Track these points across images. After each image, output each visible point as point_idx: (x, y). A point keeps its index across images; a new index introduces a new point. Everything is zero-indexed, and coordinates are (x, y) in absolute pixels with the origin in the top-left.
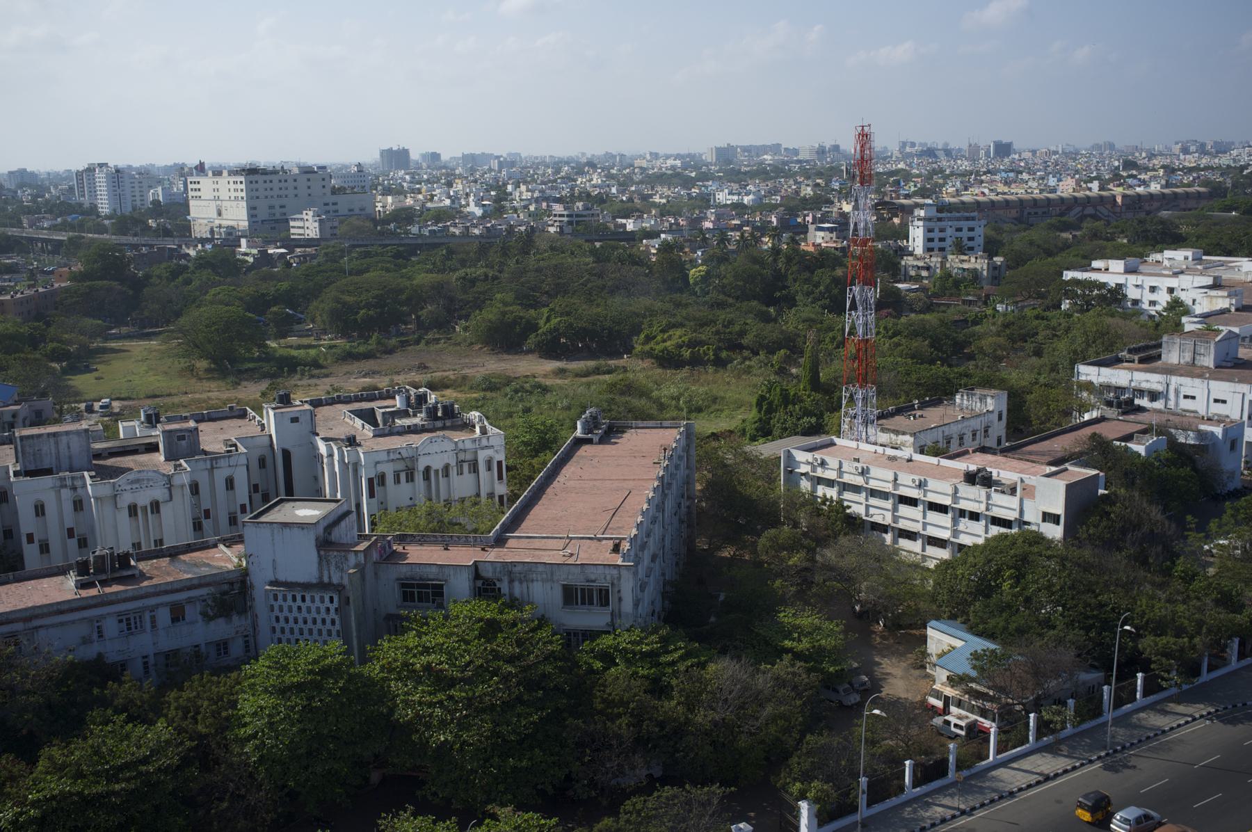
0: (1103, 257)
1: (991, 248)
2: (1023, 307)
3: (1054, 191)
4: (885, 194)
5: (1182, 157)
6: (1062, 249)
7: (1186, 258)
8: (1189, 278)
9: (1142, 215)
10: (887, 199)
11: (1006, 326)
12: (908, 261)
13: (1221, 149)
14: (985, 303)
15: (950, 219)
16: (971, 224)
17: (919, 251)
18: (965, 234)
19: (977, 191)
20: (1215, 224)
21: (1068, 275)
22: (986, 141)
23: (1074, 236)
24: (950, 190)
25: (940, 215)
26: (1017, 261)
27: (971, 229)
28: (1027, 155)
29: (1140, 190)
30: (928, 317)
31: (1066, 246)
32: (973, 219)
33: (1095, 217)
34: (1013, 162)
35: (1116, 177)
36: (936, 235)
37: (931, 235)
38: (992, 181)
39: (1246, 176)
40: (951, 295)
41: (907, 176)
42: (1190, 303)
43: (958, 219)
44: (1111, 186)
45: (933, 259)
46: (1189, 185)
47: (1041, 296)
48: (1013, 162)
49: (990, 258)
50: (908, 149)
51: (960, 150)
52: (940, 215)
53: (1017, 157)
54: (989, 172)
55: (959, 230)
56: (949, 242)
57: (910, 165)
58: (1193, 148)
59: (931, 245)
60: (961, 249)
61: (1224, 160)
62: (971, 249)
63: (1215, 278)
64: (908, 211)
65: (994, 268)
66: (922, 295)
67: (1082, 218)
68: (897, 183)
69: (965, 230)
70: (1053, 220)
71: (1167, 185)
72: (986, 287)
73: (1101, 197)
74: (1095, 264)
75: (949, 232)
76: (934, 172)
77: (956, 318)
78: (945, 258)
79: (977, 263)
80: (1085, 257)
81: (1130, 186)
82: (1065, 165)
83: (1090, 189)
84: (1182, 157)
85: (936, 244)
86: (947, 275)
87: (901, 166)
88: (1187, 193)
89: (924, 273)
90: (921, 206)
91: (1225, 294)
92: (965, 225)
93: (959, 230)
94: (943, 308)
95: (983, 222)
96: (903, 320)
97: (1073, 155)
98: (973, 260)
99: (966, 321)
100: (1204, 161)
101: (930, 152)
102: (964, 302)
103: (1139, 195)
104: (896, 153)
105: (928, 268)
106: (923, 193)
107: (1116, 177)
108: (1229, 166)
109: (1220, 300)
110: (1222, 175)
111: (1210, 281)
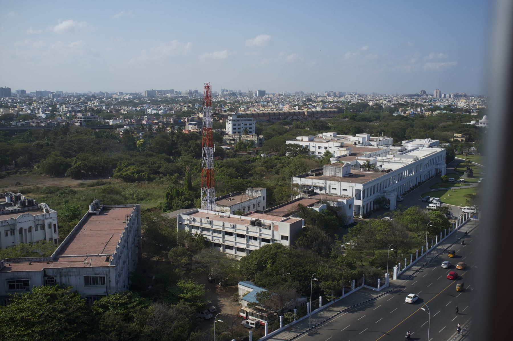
0: (300, 135)
1: (258, 132)
2: (271, 155)
3: (281, 109)
4: (216, 110)
5: (328, 97)
6: (285, 132)
7: (331, 136)
8: (332, 143)
9: (314, 119)
10: (217, 112)
11: (265, 162)
12: (226, 137)
13: (341, 95)
14: (257, 154)
15: (242, 120)
16: (250, 122)
17: (230, 133)
18: (248, 126)
19: (252, 109)
21: (288, 142)
22: (255, 90)
23: (290, 127)
24: (242, 109)
25: (238, 119)
26: (268, 137)
27: (250, 124)
28: (271, 96)
29: (313, 110)
30: (234, 159)
31: (287, 131)
32: (251, 120)
33: (297, 120)
34: (265, 98)
35: (305, 104)
36: (237, 127)
37: (235, 127)
38: (258, 106)
39: (350, 105)
40: (243, 151)
41: (225, 103)
43: (245, 120)
44: (302, 108)
45: (236, 136)
46: (331, 108)
47: (278, 150)
48: (265, 98)
49: (258, 136)
50: (225, 93)
51: (245, 93)
52: (238, 119)
53: (267, 96)
54: (257, 102)
55: (246, 125)
56: (242, 129)
57: (226, 99)
58: (331, 94)
59: (235, 131)
60: (246, 132)
61: (342, 99)
62: (251, 132)
63: (341, 143)
64: (225, 117)
65: (259, 140)
66: (232, 151)
67: (293, 120)
68: (221, 106)
69: (248, 125)
70: (282, 121)
71: (323, 108)
72: (257, 147)
73: (299, 112)
74: (298, 138)
75: (242, 125)
76: (236, 102)
77: (246, 159)
78: (240, 136)
79: (253, 138)
80: (294, 135)
81: (310, 108)
82: (285, 100)
83: (295, 109)
84: (328, 97)
85: (237, 130)
86: (241, 143)
87: (222, 99)
89: (233, 142)
90: (231, 115)
92: (248, 123)
93: (246, 125)
94: (240, 156)
95: (255, 122)
96: (224, 160)
97: (288, 96)
98: (251, 136)
99: (249, 161)
101: (234, 94)
102: (248, 153)
103: (313, 112)
104: (220, 94)
105: (234, 140)
106: (231, 110)
107: (305, 104)
109: (343, 152)
111: (339, 144)
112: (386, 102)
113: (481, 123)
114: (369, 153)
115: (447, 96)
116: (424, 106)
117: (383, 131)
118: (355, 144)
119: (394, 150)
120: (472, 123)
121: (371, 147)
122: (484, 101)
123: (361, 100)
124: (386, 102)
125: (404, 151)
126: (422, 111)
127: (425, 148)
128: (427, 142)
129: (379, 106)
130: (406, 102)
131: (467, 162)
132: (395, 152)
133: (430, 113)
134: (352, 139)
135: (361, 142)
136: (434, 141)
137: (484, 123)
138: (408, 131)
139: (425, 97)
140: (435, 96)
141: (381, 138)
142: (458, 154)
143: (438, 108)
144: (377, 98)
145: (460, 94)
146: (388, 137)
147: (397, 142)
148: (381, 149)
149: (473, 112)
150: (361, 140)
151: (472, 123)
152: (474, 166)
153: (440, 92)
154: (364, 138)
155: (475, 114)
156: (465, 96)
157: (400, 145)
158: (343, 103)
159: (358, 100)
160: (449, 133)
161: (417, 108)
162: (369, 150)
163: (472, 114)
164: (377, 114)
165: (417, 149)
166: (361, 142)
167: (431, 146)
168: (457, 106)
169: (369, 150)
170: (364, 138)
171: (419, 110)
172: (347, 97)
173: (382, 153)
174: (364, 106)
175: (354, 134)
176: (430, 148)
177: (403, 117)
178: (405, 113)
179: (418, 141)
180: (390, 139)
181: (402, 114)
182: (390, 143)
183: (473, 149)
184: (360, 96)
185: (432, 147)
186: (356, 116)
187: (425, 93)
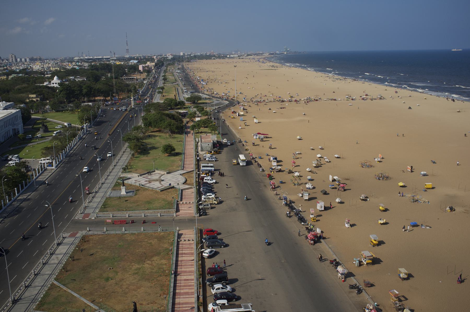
113: (53, 84)
115: (23, 60)
120: (45, 84)
122: (58, 63)
131: (42, 119)
133: (5, 77)
136: (9, 103)
137: (56, 83)
140: (11, 61)
142: (35, 113)
143: (14, 72)
145: (35, 58)
149: (47, 74)
151: (45, 84)
152: (49, 122)
155: (49, 76)
156: (40, 59)
160: (24, 95)
163: (46, 76)
167: (6, 108)
168: (32, 69)
176: (5, 111)
183: (47, 107)
185: (7, 109)
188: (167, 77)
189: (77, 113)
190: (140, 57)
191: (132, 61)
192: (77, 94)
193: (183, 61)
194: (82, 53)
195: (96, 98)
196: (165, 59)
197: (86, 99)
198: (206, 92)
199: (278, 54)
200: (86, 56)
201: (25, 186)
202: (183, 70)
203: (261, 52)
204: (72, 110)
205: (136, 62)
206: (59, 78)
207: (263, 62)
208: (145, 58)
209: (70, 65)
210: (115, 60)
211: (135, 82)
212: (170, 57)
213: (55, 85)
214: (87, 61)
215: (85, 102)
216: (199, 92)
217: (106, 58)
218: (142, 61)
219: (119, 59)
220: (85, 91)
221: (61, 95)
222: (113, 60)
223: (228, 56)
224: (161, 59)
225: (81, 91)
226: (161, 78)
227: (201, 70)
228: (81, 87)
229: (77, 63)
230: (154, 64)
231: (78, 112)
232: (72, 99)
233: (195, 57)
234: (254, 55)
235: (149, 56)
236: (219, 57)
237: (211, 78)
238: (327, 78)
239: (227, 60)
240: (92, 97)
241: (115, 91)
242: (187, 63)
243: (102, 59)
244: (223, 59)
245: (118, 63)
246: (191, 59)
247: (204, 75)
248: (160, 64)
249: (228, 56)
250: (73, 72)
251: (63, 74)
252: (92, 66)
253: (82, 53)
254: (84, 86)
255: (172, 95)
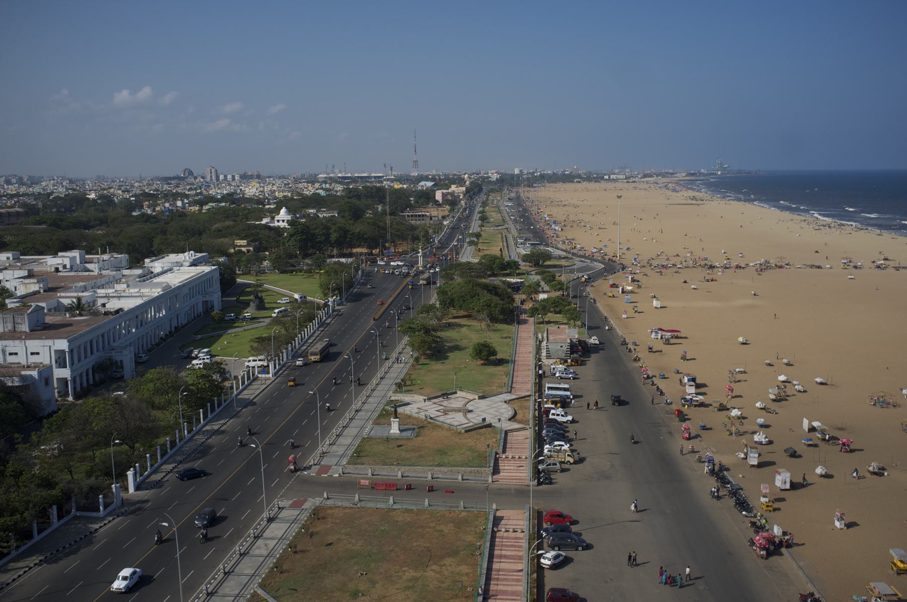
5: (6, 187)
7: (8, 258)
8: (11, 272)
13: (34, 181)
20: (30, 234)
39: (51, 200)
42: (13, 290)
46: (11, 207)
58: (14, 181)
61: (37, 189)
63: (29, 271)
84: (6, 187)
88: (9, 213)
91: (35, 281)
100: (22, 190)
108: (39, 194)
109: (32, 286)
110: (35, 199)
111: (26, 273)
112: (120, 192)
113: (278, 221)
114: (81, 284)
115: (229, 177)
116: (187, 196)
117: (110, 244)
118: (57, 270)
119: (131, 276)
120: (264, 221)
121: (87, 273)
123: (74, 190)
124: (120, 192)
125: (148, 276)
126: (183, 204)
127: (185, 269)
128: (188, 257)
129: (107, 200)
130: (157, 190)
131: (254, 285)
132: (131, 278)
133: (197, 208)
134: (51, 262)
135: (68, 266)
136: (199, 255)
137: (283, 221)
138: (157, 241)
139: (191, 180)
140: (208, 179)
141: (106, 257)
143: (212, 199)
144: (105, 185)
146: (121, 253)
147: (136, 261)
148: (104, 276)
150: (67, 262)
151: (264, 221)
152: (267, 290)
153: (216, 171)
154: (73, 259)
155: (272, 207)
156: (258, 177)
157: (142, 267)
158: (38, 196)
159: (67, 189)
160: (226, 240)
161: (175, 200)
162: (83, 279)
163: (267, 207)
164: (101, 215)
165: (170, 270)
166: (68, 266)
167: (194, 264)
168: (244, 194)
169: (83, 279)
170: (73, 259)
171: (179, 203)
172: (47, 186)
173: (107, 283)
174: (77, 200)
175: (55, 254)
176: (193, 268)
177: (150, 216)
178: (154, 210)
179: (173, 257)
180: (123, 257)
181: (149, 212)
182: (124, 263)
183: (265, 263)
184: (71, 181)
186: (61, 220)
187: (191, 173)
188: (488, 214)
189: (317, 276)
190: (439, 175)
191: (422, 183)
192: (320, 242)
193: (518, 185)
194: (333, 167)
195: (355, 250)
196: (486, 180)
197: (335, 252)
198: (560, 245)
199: (704, 175)
200: (340, 172)
201: (218, 407)
202: (518, 201)
203: (671, 171)
204: (309, 271)
205: (430, 184)
206: (289, 211)
207: (674, 190)
208: (447, 177)
209: (310, 188)
210: (392, 181)
211: (428, 221)
212: (495, 177)
213: (282, 225)
214: (341, 180)
215: (333, 257)
216: (547, 245)
217: (375, 177)
218: (441, 183)
219: (399, 179)
220: (334, 236)
221: (290, 243)
222: (388, 180)
223: (606, 177)
224: (478, 179)
225: (327, 235)
226: (476, 216)
227: (553, 203)
228: (327, 228)
229: (324, 185)
230: (464, 189)
231: (321, 274)
232: (310, 252)
233: (542, 177)
234: (657, 176)
235: (454, 175)
236: (589, 178)
237: (572, 217)
238: (804, 224)
239: (603, 184)
240: (347, 248)
241: (389, 237)
242: (527, 189)
243: (369, 177)
244: (596, 182)
245: (397, 186)
246: (533, 181)
247: (559, 213)
248: (476, 189)
249: (606, 177)
250: (316, 201)
251: (296, 204)
252: (350, 191)
253: (333, 167)
254: (334, 227)
255: (495, 248)
